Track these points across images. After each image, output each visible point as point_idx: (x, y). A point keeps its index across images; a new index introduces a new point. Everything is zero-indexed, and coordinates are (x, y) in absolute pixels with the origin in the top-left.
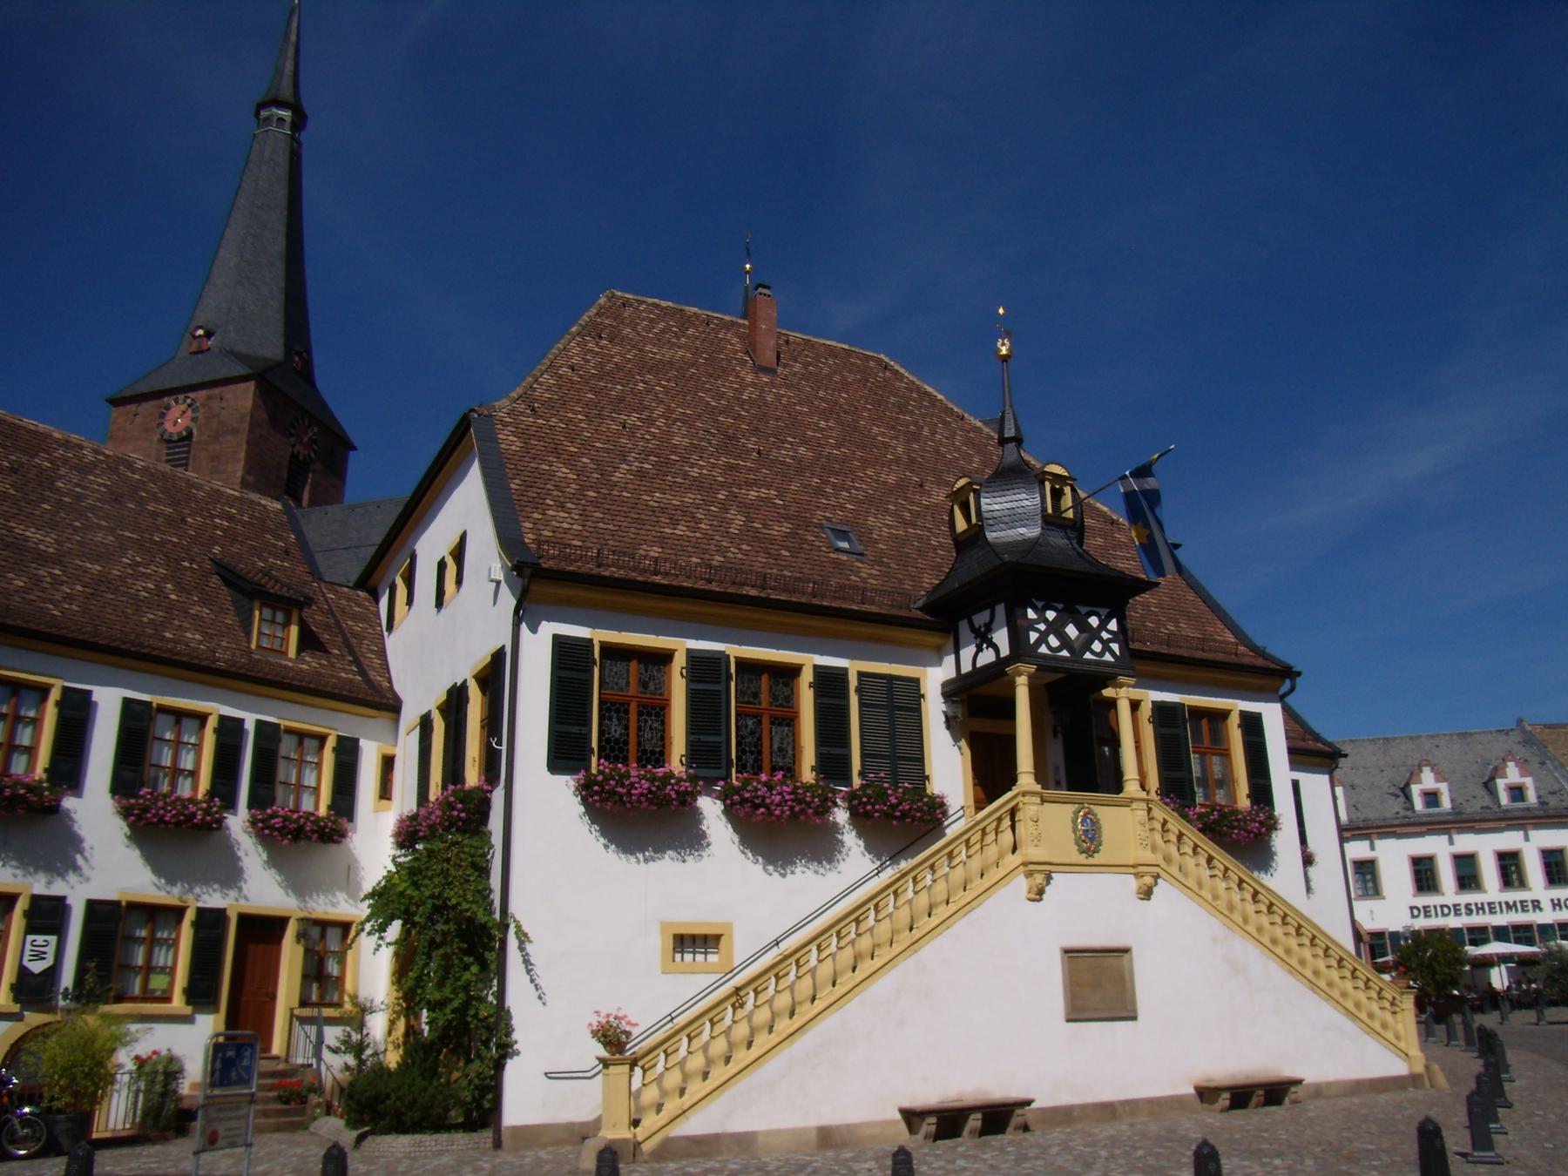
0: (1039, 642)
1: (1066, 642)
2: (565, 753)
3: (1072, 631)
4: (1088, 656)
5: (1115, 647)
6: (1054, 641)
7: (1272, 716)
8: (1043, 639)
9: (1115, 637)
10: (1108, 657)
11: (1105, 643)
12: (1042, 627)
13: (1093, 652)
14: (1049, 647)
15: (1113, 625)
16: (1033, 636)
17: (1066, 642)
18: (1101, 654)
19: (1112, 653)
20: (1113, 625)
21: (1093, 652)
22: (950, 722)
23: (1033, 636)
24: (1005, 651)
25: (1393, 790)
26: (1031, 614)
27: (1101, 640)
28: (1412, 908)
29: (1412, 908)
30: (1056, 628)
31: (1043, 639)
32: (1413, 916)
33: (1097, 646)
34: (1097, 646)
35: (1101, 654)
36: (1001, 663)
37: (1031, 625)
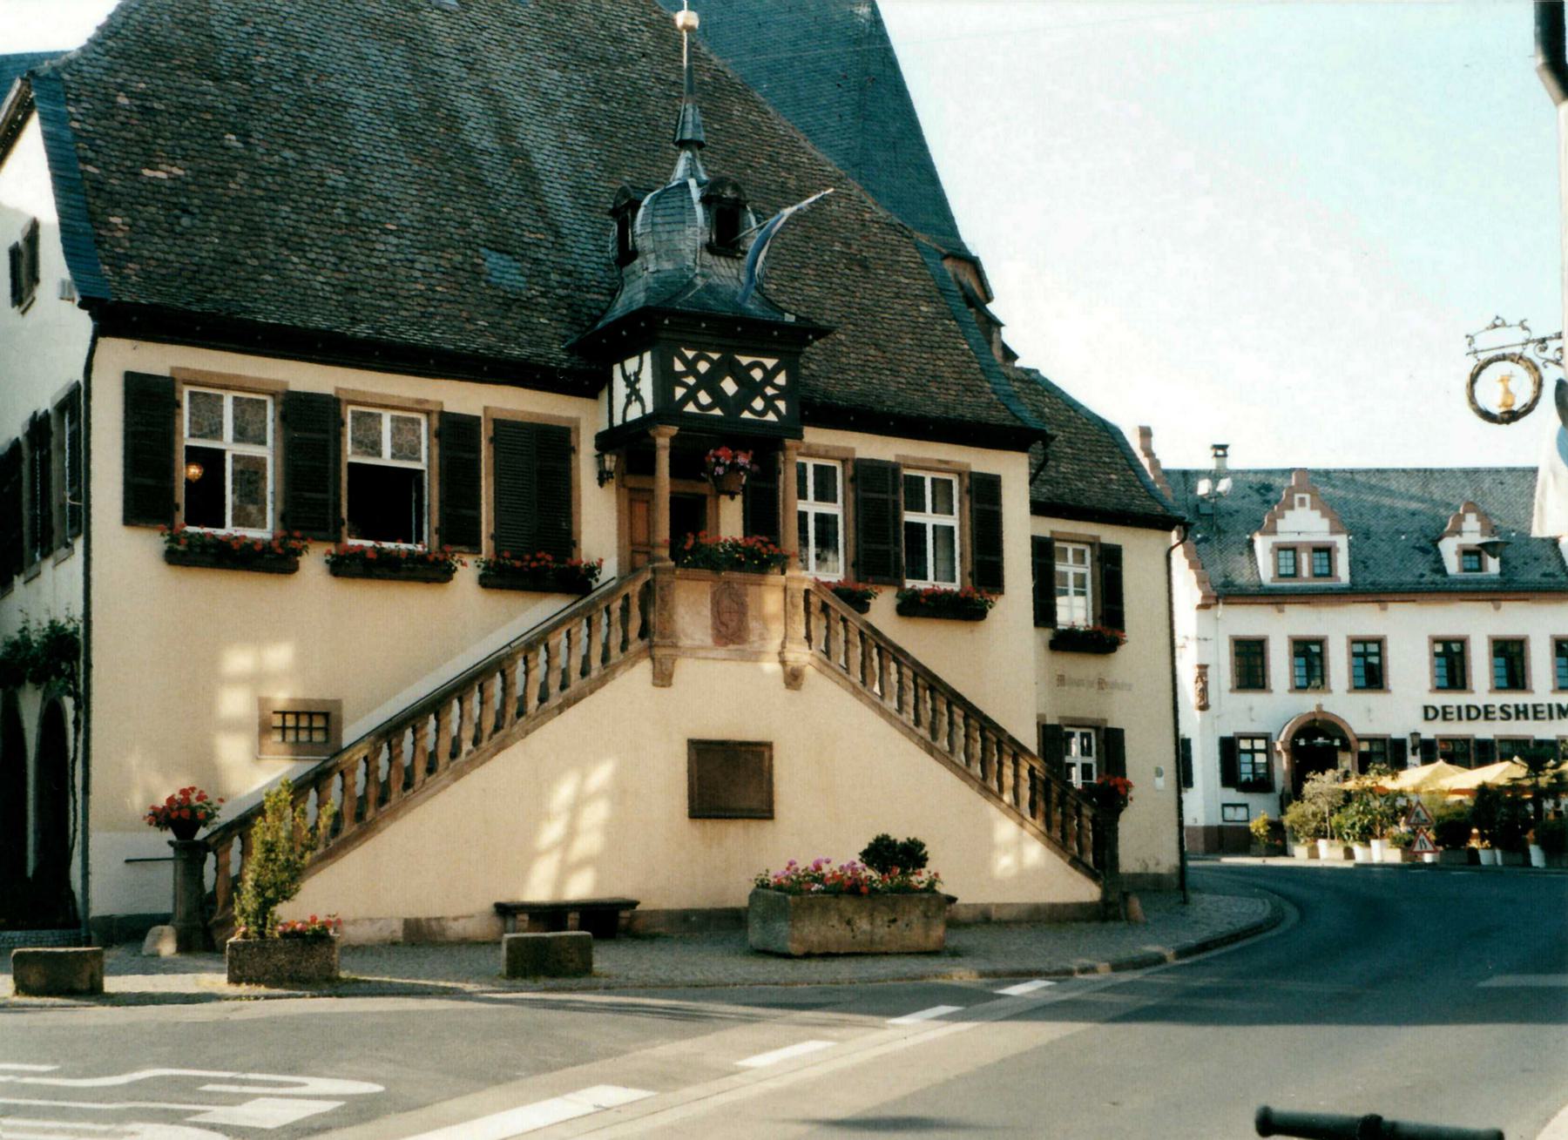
0: (685, 400)
1: (719, 397)
2: (143, 506)
3: (729, 386)
4: (746, 415)
5: (781, 405)
6: (704, 398)
7: (1013, 473)
8: (691, 395)
9: (783, 393)
10: (771, 417)
11: (770, 404)
12: (691, 381)
13: (753, 411)
14: (697, 404)
15: (781, 379)
16: (680, 392)
17: (719, 397)
18: (763, 413)
19: (777, 411)
20: (781, 379)
21: (753, 411)
22: (603, 478)
23: (680, 392)
24: (649, 409)
25: (1423, 542)
26: (679, 366)
27: (764, 397)
28: (1426, 708)
29: (1426, 708)
30: (710, 382)
31: (691, 395)
32: (1426, 718)
33: (758, 404)
34: (758, 404)
35: (763, 413)
36: (646, 420)
37: (677, 379)
